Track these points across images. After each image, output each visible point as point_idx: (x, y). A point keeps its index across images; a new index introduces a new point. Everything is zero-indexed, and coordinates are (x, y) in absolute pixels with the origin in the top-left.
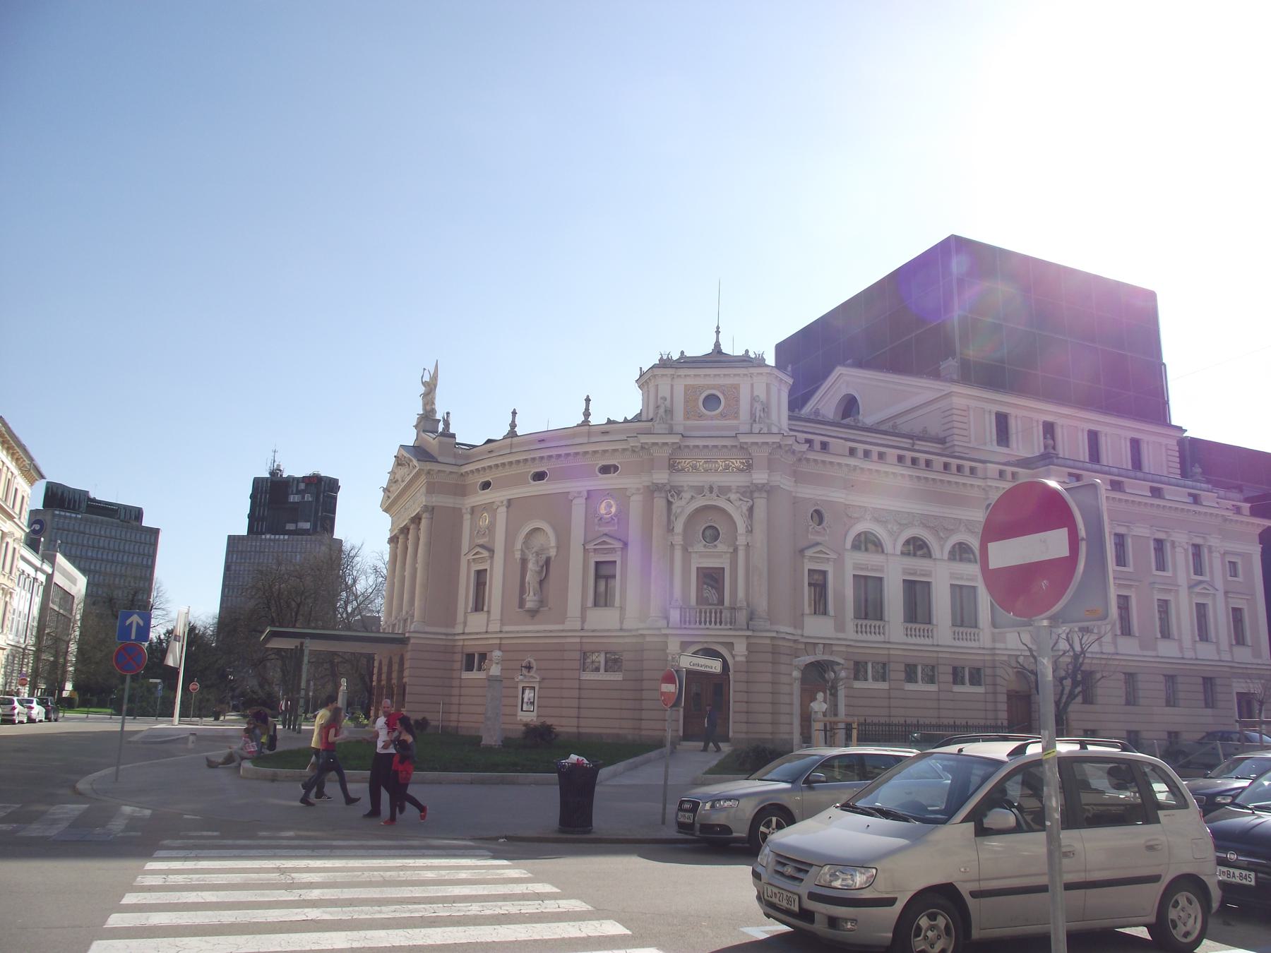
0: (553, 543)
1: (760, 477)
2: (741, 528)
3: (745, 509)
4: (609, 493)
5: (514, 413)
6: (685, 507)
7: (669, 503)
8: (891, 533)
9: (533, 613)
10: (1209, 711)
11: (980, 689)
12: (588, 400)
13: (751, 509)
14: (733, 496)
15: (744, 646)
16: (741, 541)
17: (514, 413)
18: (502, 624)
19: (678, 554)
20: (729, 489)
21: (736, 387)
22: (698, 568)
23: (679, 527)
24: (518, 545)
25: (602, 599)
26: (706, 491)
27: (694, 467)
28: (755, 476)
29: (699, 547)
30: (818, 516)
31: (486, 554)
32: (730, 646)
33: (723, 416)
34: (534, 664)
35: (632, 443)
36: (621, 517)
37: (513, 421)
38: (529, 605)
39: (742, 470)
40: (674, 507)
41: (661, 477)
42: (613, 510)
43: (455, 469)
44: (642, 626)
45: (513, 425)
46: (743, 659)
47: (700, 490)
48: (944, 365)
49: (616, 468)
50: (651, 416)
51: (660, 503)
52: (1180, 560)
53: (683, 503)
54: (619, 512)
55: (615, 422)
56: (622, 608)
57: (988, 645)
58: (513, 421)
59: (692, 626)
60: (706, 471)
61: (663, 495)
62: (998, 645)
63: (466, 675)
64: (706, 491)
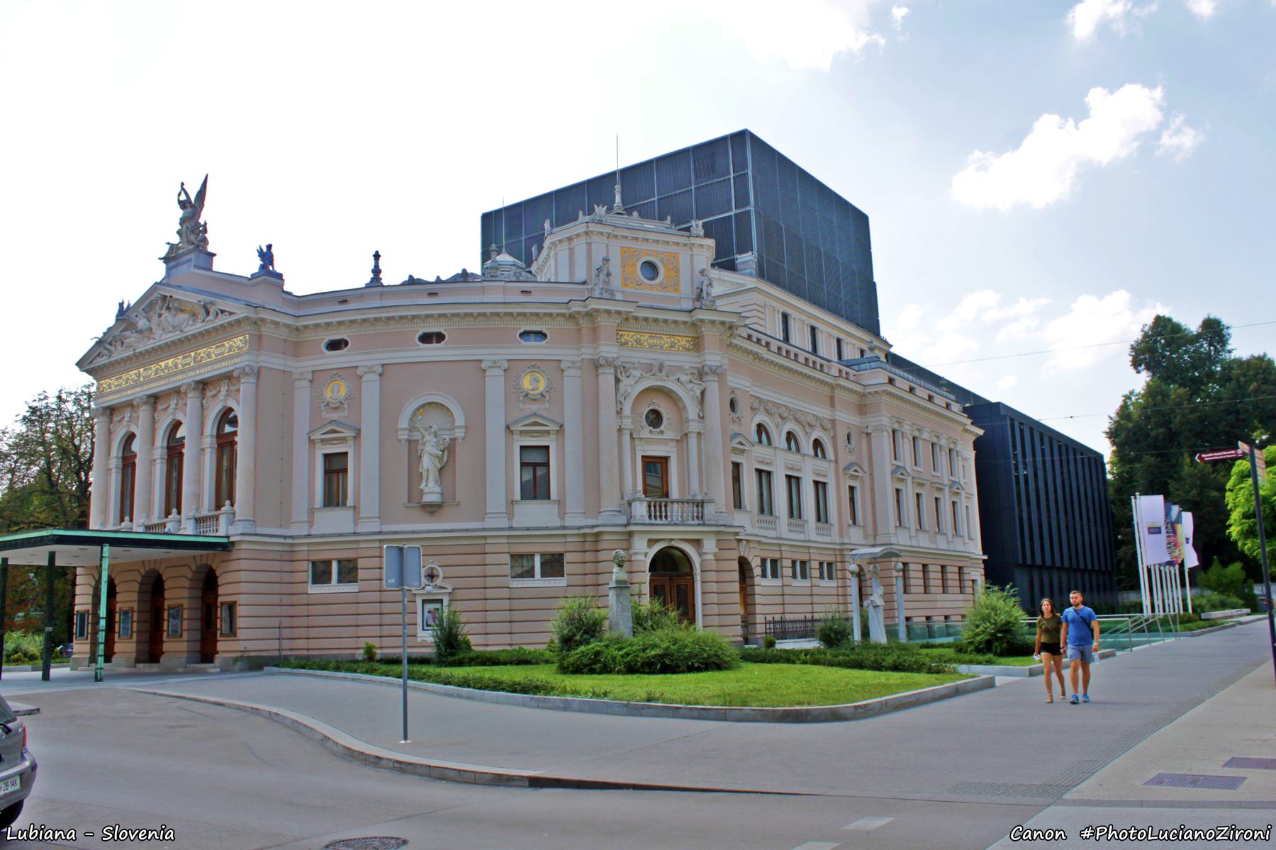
0: (460, 420)
1: (713, 357)
2: (692, 411)
3: (698, 393)
4: (534, 365)
5: (377, 256)
6: (634, 386)
7: (617, 380)
8: (777, 426)
9: (432, 509)
10: (961, 596)
11: (833, 584)
12: (377, 256)
13: (703, 393)
14: (684, 378)
15: (714, 542)
16: (694, 427)
17: (377, 256)
18: (382, 523)
19: (626, 438)
20: (679, 368)
21: (675, 257)
22: (643, 457)
23: (627, 411)
24: (404, 423)
25: (536, 489)
26: (655, 369)
27: (638, 342)
28: (707, 357)
29: (646, 431)
30: (733, 405)
31: (348, 433)
32: (697, 543)
33: (663, 286)
34: (440, 572)
35: (575, 308)
36: (553, 393)
37: (377, 266)
38: (427, 499)
39: (688, 350)
40: (622, 386)
41: (608, 350)
42: (542, 386)
43: (290, 321)
44: (591, 522)
45: (377, 271)
46: (712, 557)
47: (649, 368)
48: (740, 258)
49: (542, 335)
50: (581, 275)
51: (607, 379)
52: (943, 459)
53: (631, 381)
54: (549, 389)
55: (420, 282)
56: (561, 503)
57: (838, 540)
58: (377, 266)
59: (658, 521)
60: (651, 347)
61: (612, 371)
62: (846, 541)
63: (314, 589)
64: (655, 369)
